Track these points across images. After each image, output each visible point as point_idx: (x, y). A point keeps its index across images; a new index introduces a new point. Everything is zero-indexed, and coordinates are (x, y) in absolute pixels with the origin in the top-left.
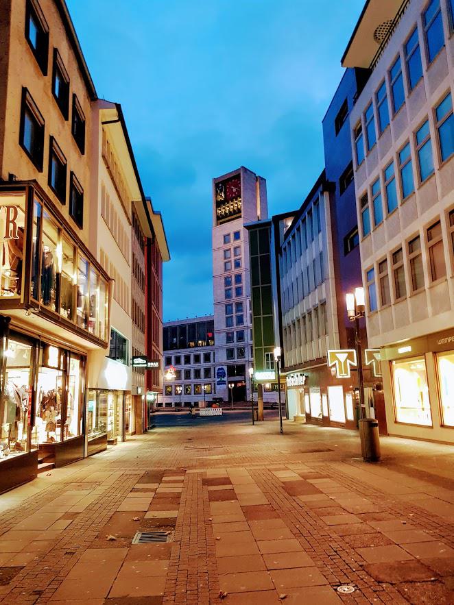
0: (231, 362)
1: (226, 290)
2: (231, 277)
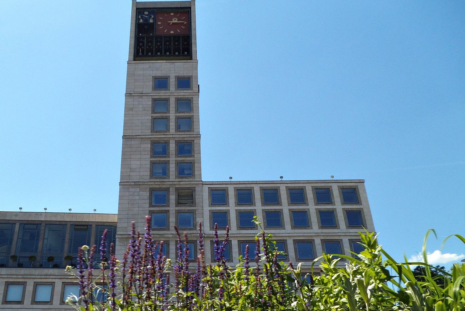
2: (167, 143)
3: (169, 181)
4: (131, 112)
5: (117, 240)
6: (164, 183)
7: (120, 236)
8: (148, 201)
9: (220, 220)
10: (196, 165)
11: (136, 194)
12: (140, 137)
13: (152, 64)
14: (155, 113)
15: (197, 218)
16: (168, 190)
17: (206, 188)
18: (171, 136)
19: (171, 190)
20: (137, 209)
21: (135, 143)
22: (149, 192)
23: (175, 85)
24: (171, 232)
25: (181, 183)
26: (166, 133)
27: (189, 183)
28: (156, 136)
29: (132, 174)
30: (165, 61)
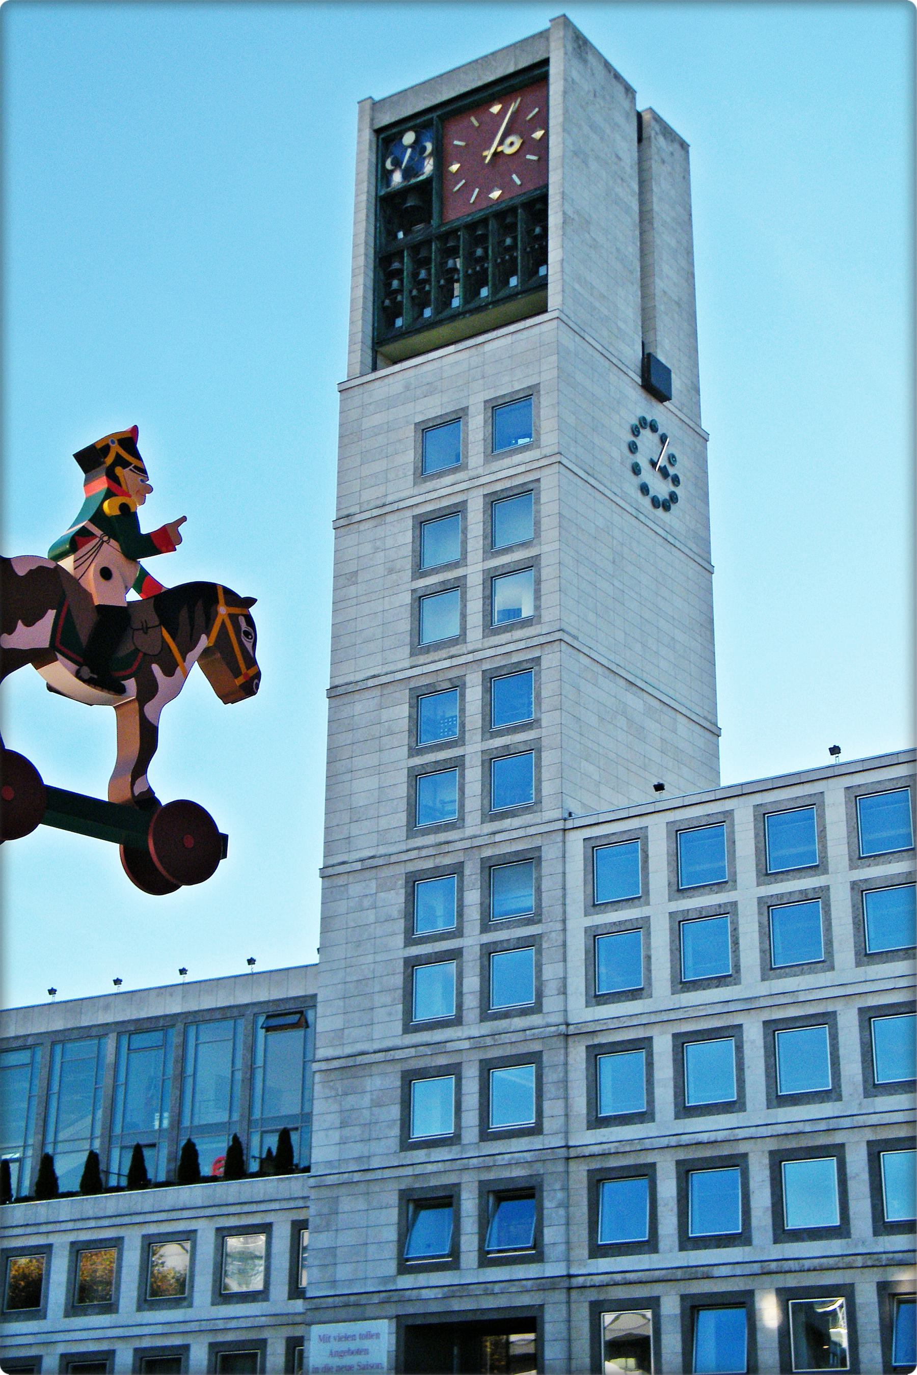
0: (430, 1291)
1: (416, 776)
2: (457, 686)
3: (462, 836)
4: (352, 591)
5: (317, 1078)
6: (446, 848)
7: (324, 1066)
8: (400, 925)
9: (613, 965)
10: (547, 757)
11: (367, 903)
12: (376, 681)
13: (411, 373)
15: (544, 966)
16: (458, 869)
18: (470, 658)
19: (467, 872)
20: (370, 958)
21: (361, 707)
22: (403, 891)
23: (485, 440)
25: (498, 838)
26: (454, 651)
27: (521, 833)
28: (426, 669)
29: (355, 830)
30: (451, 349)
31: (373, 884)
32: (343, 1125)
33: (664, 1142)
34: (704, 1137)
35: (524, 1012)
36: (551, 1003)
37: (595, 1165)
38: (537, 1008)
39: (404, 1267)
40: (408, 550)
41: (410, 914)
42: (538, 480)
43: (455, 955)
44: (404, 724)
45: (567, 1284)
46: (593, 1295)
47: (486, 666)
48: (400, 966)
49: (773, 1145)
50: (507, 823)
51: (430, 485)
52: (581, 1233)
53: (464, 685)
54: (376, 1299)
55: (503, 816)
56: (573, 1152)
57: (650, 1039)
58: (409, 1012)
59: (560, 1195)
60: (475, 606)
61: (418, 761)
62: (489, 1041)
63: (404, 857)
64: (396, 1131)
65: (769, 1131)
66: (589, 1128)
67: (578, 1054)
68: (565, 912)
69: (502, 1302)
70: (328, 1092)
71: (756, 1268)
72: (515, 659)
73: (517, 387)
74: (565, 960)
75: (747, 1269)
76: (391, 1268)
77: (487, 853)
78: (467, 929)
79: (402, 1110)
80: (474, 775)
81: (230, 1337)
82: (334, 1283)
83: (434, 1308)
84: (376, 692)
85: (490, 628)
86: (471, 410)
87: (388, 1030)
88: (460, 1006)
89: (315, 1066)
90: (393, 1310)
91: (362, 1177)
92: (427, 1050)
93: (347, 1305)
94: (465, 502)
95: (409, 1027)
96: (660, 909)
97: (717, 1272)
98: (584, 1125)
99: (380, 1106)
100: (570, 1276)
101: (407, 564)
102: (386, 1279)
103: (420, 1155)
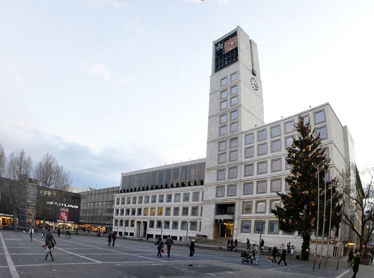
5: (205, 171)
8: (218, 149)
14: (221, 99)
17: (243, 135)
18: (228, 110)
19: (227, 141)
21: (213, 118)
24: (226, 164)
31: (214, 143)
32: (209, 177)
33: (255, 179)
34: (261, 178)
35: (235, 160)
36: (239, 159)
37: (245, 182)
38: (237, 160)
39: (216, 197)
40: (219, 96)
41: (219, 147)
42: (237, 84)
43: (225, 153)
44: (219, 120)
45: (240, 199)
46: (243, 201)
47: (230, 111)
48: (217, 155)
49: (271, 178)
50: (234, 133)
51: (222, 87)
52: (242, 192)
53: (227, 114)
54: (212, 201)
55: (233, 132)
56: (241, 181)
57: (254, 163)
58: (219, 161)
59: (239, 187)
60: (229, 103)
61: (220, 126)
62: (230, 165)
63: (218, 139)
64: (216, 178)
65: (271, 176)
66: (244, 177)
67: (243, 166)
68: (241, 145)
69: (230, 201)
70: (207, 173)
71: (267, 197)
72: (234, 109)
73: (234, 72)
74: (241, 152)
75: (266, 197)
76: (215, 196)
77: (230, 138)
78: (227, 149)
79: (217, 175)
80: (228, 126)
81: (194, 206)
82: (207, 199)
83: (220, 202)
84: (215, 116)
85: (231, 106)
86: (228, 76)
87: (215, 164)
88: (226, 160)
89: (205, 169)
90: (215, 202)
91: (211, 185)
92: (221, 167)
93: (209, 202)
94: (227, 89)
95: (218, 163)
96: (256, 144)
97: (261, 197)
98: (243, 177)
99: (214, 174)
100: (240, 198)
101: (219, 98)
102: (214, 198)
103: (220, 181)
